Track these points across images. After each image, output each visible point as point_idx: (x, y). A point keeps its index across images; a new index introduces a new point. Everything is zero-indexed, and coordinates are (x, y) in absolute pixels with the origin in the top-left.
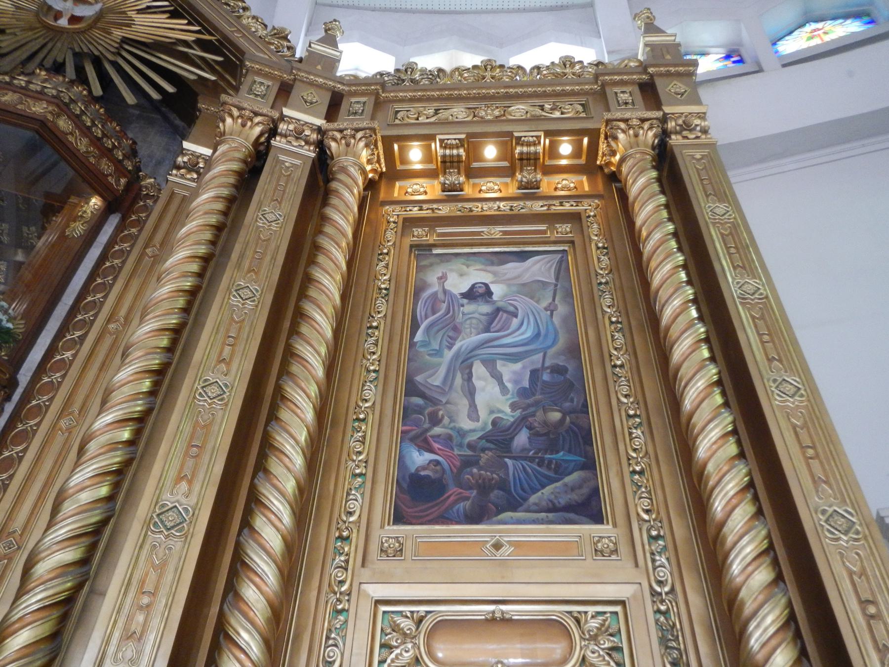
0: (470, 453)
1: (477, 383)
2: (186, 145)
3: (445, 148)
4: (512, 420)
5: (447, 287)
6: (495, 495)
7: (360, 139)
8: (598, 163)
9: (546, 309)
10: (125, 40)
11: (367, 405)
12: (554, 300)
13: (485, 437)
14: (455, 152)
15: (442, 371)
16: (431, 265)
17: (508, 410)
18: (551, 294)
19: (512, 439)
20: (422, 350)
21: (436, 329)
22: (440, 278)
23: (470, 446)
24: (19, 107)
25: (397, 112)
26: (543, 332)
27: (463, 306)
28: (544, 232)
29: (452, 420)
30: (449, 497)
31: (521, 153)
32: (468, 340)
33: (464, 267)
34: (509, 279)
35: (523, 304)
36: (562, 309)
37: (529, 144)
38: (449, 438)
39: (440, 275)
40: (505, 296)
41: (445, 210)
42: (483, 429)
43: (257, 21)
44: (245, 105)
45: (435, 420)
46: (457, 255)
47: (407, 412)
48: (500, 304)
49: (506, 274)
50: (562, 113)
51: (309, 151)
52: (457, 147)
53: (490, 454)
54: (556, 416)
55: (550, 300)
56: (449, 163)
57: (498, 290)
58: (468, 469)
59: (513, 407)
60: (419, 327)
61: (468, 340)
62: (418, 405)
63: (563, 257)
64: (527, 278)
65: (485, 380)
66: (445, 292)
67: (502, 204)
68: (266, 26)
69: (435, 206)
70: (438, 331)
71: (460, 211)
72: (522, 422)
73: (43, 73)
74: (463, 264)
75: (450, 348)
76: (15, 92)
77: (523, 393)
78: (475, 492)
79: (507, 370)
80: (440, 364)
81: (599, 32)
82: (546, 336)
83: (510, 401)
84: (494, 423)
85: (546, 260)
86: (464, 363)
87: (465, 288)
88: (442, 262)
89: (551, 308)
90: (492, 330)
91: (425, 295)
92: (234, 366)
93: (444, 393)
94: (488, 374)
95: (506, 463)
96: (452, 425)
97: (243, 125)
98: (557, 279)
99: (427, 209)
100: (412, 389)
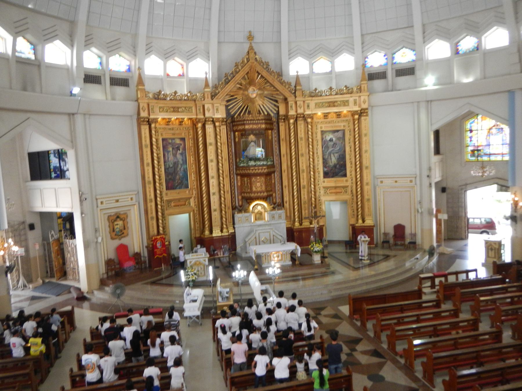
32: (330, 150)
35: (338, 142)
36: (343, 143)
38: (329, 167)
40: (335, 141)
45: (327, 164)
47: (323, 163)
54: (342, 162)
57: (334, 139)
61: (330, 150)
66: (326, 140)
72: (338, 163)
77: (338, 159)
86: (330, 154)
89: (342, 143)
100: (323, 159)
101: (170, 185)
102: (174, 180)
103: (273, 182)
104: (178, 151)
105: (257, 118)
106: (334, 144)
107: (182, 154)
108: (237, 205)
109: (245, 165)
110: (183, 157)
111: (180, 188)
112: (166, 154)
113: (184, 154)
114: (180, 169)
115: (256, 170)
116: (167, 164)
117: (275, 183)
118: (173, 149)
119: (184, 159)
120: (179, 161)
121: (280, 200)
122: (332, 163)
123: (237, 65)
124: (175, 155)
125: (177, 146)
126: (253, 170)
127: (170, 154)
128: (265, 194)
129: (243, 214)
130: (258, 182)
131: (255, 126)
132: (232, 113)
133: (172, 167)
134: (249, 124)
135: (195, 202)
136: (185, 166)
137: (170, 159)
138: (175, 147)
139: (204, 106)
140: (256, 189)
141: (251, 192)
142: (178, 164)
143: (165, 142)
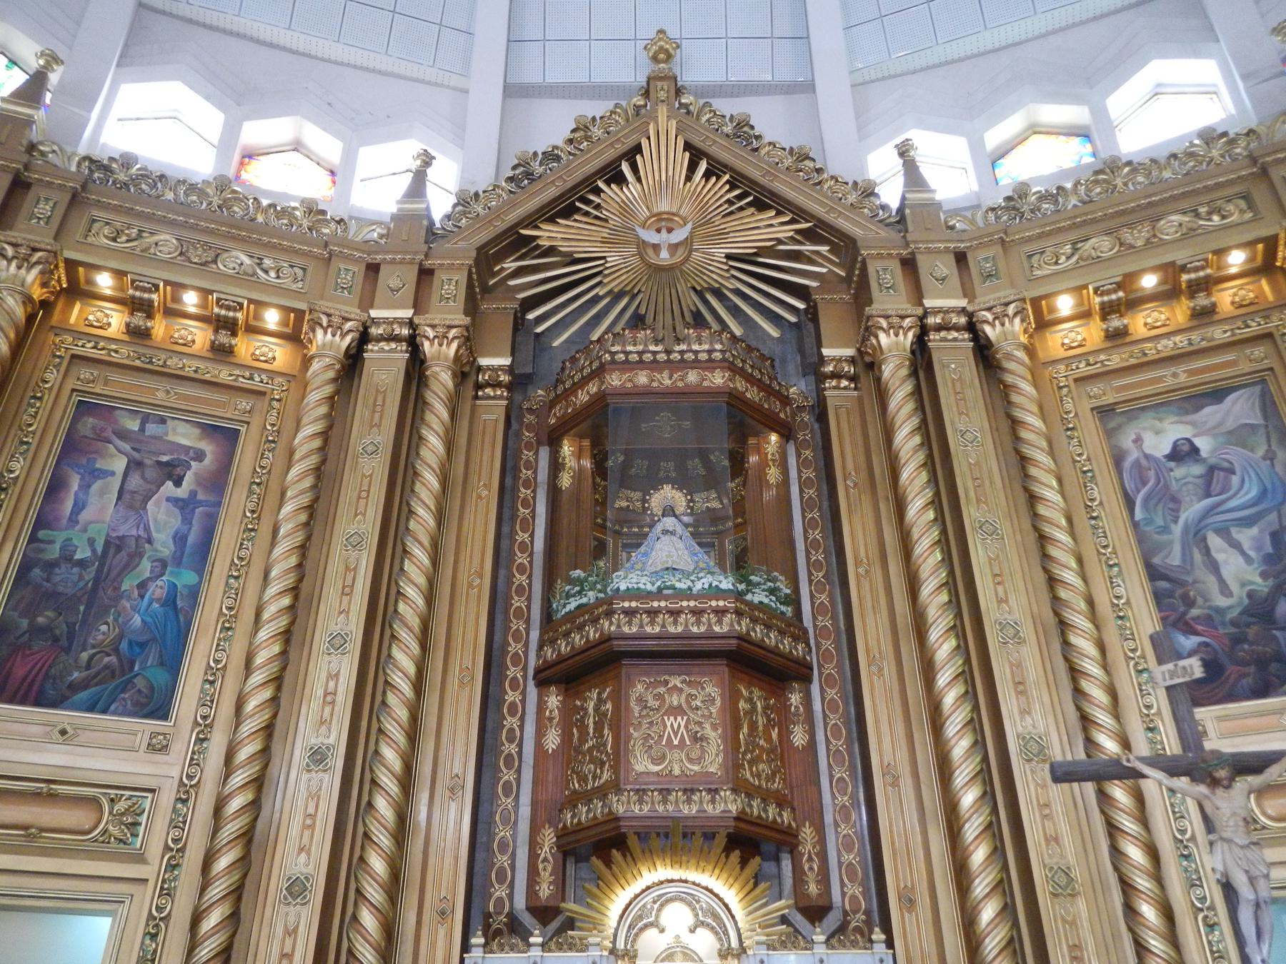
0: (1233, 630)
1: (1220, 557)
2: (825, 352)
3: (1102, 295)
4: (1266, 590)
5: (1147, 451)
6: (1274, 667)
7: (1015, 315)
8: (1278, 264)
9: (1264, 458)
10: (729, 257)
11: (1122, 601)
12: (1270, 446)
13: (1245, 612)
14: (1114, 297)
15: (1177, 549)
16: (1120, 426)
17: (1259, 580)
18: (1263, 439)
19: (1273, 610)
20: (1147, 529)
21: (1153, 502)
22: (1135, 441)
23: (1233, 623)
24: (705, 384)
25: (1030, 257)
26: (1269, 486)
27: (1171, 470)
28: (1233, 363)
29: (1206, 600)
30: (1229, 675)
31: (1190, 281)
32: (1192, 509)
33: (1157, 423)
34: (1214, 428)
35: (1235, 455)
37: (1197, 269)
38: (1209, 617)
39: (1134, 437)
40: (1214, 450)
41: (1116, 360)
42: (1239, 604)
43: (837, 181)
44: (890, 312)
45: (1190, 603)
46: (1143, 409)
47: (1158, 597)
48: (1213, 461)
49: (1206, 422)
50: (1224, 217)
51: (963, 340)
52: (1115, 291)
53: (1256, 628)
55: (1265, 447)
56: (1107, 311)
57: (1203, 444)
58: (1239, 647)
59: (1264, 575)
60: (1134, 503)
62: (1166, 590)
63: (1263, 388)
64: (1230, 424)
65: (1225, 552)
66: (1147, 456)
67: (1178, 339)
68: (847, 184)
69: (1102, 357)
70: (1156, 505)
71: (1131, 357)
73: (691, 331)
74: (1154, 419)
75: (1176, 521)
76: (692, 368)
77: (1269, 559)
78: (1252, 669)
79: (1246, 536)
80: (1171, 543)
81: (1213, 30)
82: (1274, 490)
83: (1259, 570)
84: (1250, 595)
85: (1246, 396)
86: (1196, 536)
87: (1166, 448)
88: (1130, 420)
90: (1213, 494)
91: (1127, 464)
92: (1012, 601)
93: (1188, 573)
94: (1226, 545)
95: (1275, 638)
96: (1207, 604)
97: (897, 335)
98: (1266, 417)
99: (1096, 363)
100: (1154, 574)
101: (19, 672)
102: (66, 642)
103: (799, 737)
104: (169, 484)
105: (683, 347)
106: (1212, 469)
107: (185, 506)
108: (520, 902)
109: (590, 597)
110: (187, 520)
111: (91, 709)
112: (75, 483)
113: (197, 510)
114: (143, 586)
115: (653, 613)
116: (60, 537)
117: (812, 743)
118: (134, 465)
119: (192, 539)
120: (150, 541)
121: (854, 890)
122: (1225, 590)
123: (582, 128)
124: (132, 501)
125: (165, 459)
126: (630, 613)
127: (102, 493)
128: (729, 805)
129: (536, 952)
130: (677, 711)
131: (665, 380)
132: (539, 330)
133: (82, 564)
134: (627, 365)
135: (173, 825)
136: (189, 577)
137: (84, 516)
138: (148, 462)
139: (373, 269)
140: (655, 761)
141: (615, 786)
142: (138, 555)
143: (91, 421)
